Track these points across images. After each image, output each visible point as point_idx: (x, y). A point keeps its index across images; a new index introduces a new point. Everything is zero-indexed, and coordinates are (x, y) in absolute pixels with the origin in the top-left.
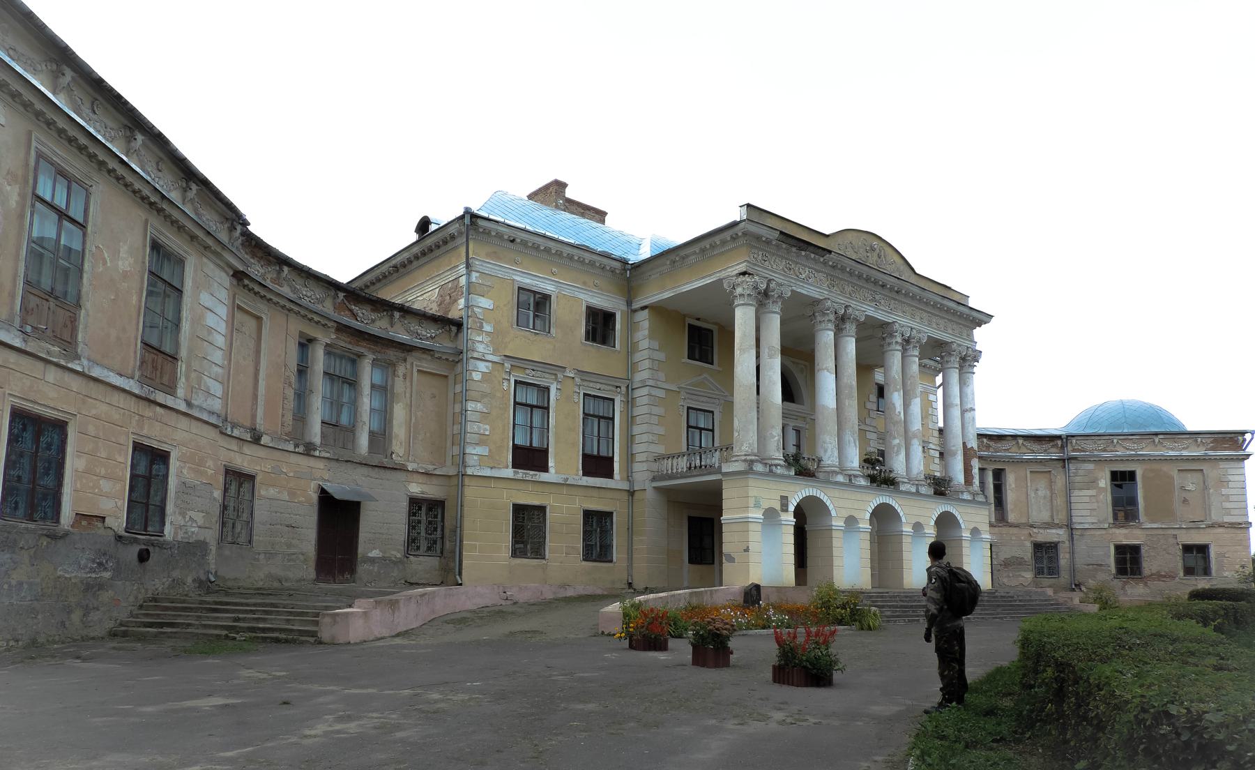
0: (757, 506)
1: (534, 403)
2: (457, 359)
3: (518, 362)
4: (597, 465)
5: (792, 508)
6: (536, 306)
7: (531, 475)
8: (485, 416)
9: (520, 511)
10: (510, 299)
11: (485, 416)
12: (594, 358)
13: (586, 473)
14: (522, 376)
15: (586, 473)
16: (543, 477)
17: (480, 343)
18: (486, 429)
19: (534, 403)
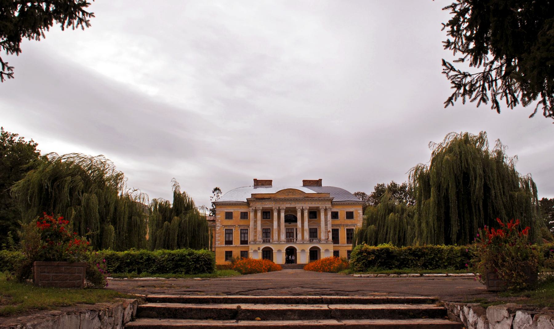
0: (252, 249)
1: (229, 232)
2: (215, 227)
3: (225, 226)
4: (244, 242)
5: (261, 249)
6: (229, 216)
7: (228, 245)
8: (219, 236)
9: (227, 252)
10: (224, 215)
11: (219, 236)
12: (243, 222)
13: (241, 244)
14: (226, 228)
15: (241, 244)
16: (231, 246)
17: (218, 224)
18: (219, 238)
19: (229, 232)
